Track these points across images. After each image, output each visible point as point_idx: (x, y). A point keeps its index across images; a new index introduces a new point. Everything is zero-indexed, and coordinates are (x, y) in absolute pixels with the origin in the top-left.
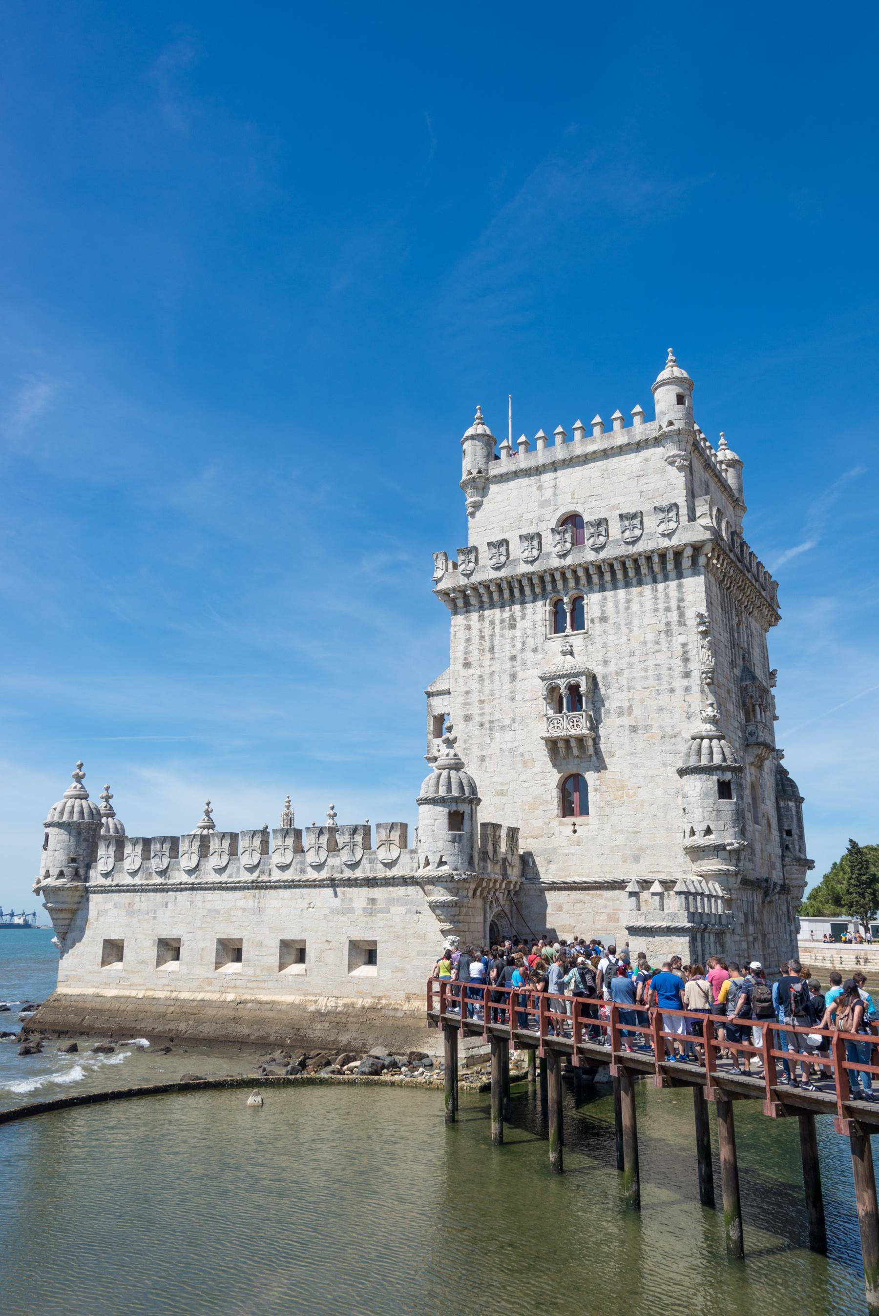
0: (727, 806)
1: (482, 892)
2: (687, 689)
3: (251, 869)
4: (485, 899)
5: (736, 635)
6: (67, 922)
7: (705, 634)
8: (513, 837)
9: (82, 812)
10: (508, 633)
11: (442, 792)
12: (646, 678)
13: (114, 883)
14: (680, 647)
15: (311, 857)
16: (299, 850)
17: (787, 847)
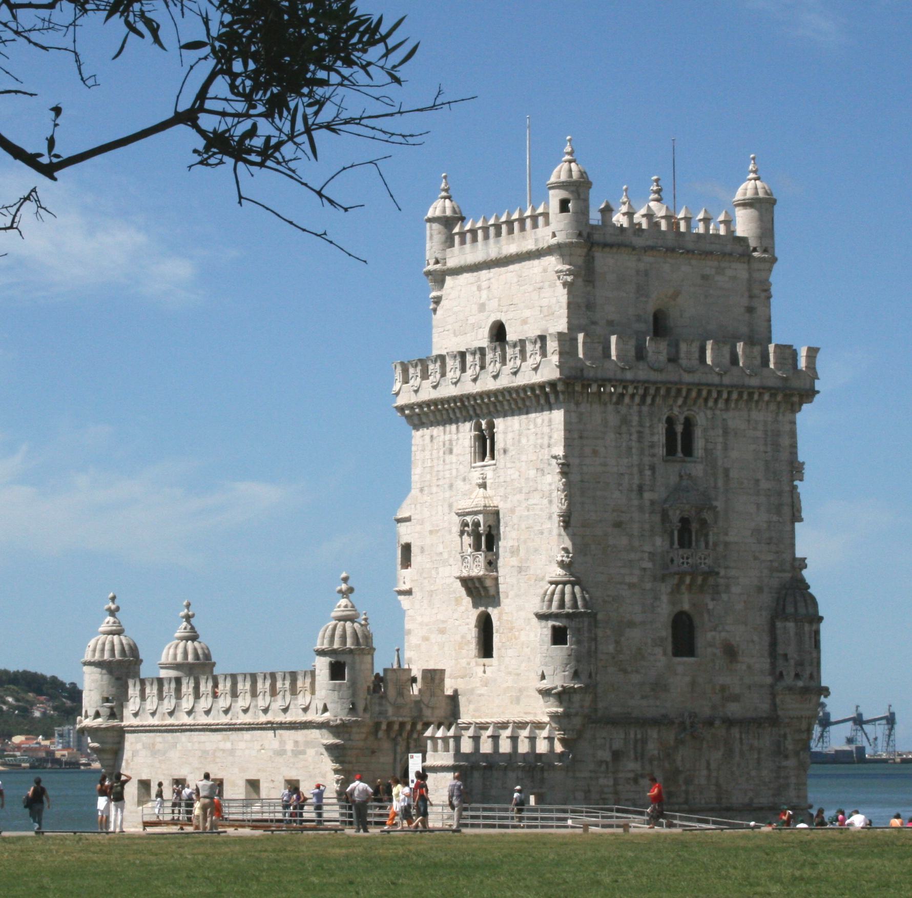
0: (561, 651)
1: (388, 737)
2: (550, 531)
3: (226, 711)
4: (394, 739)
5: (661, 451)
6: (111, 763)
7: (564, 474)
8: (433, 679)
9: (112, 650)
10: (448, 458)
11: (326, 646)
12: (528, 517)
13: (140, 723)
14: (548, 487)
15: (262, 702)
16: (254, 694)
17: (781, 674)
